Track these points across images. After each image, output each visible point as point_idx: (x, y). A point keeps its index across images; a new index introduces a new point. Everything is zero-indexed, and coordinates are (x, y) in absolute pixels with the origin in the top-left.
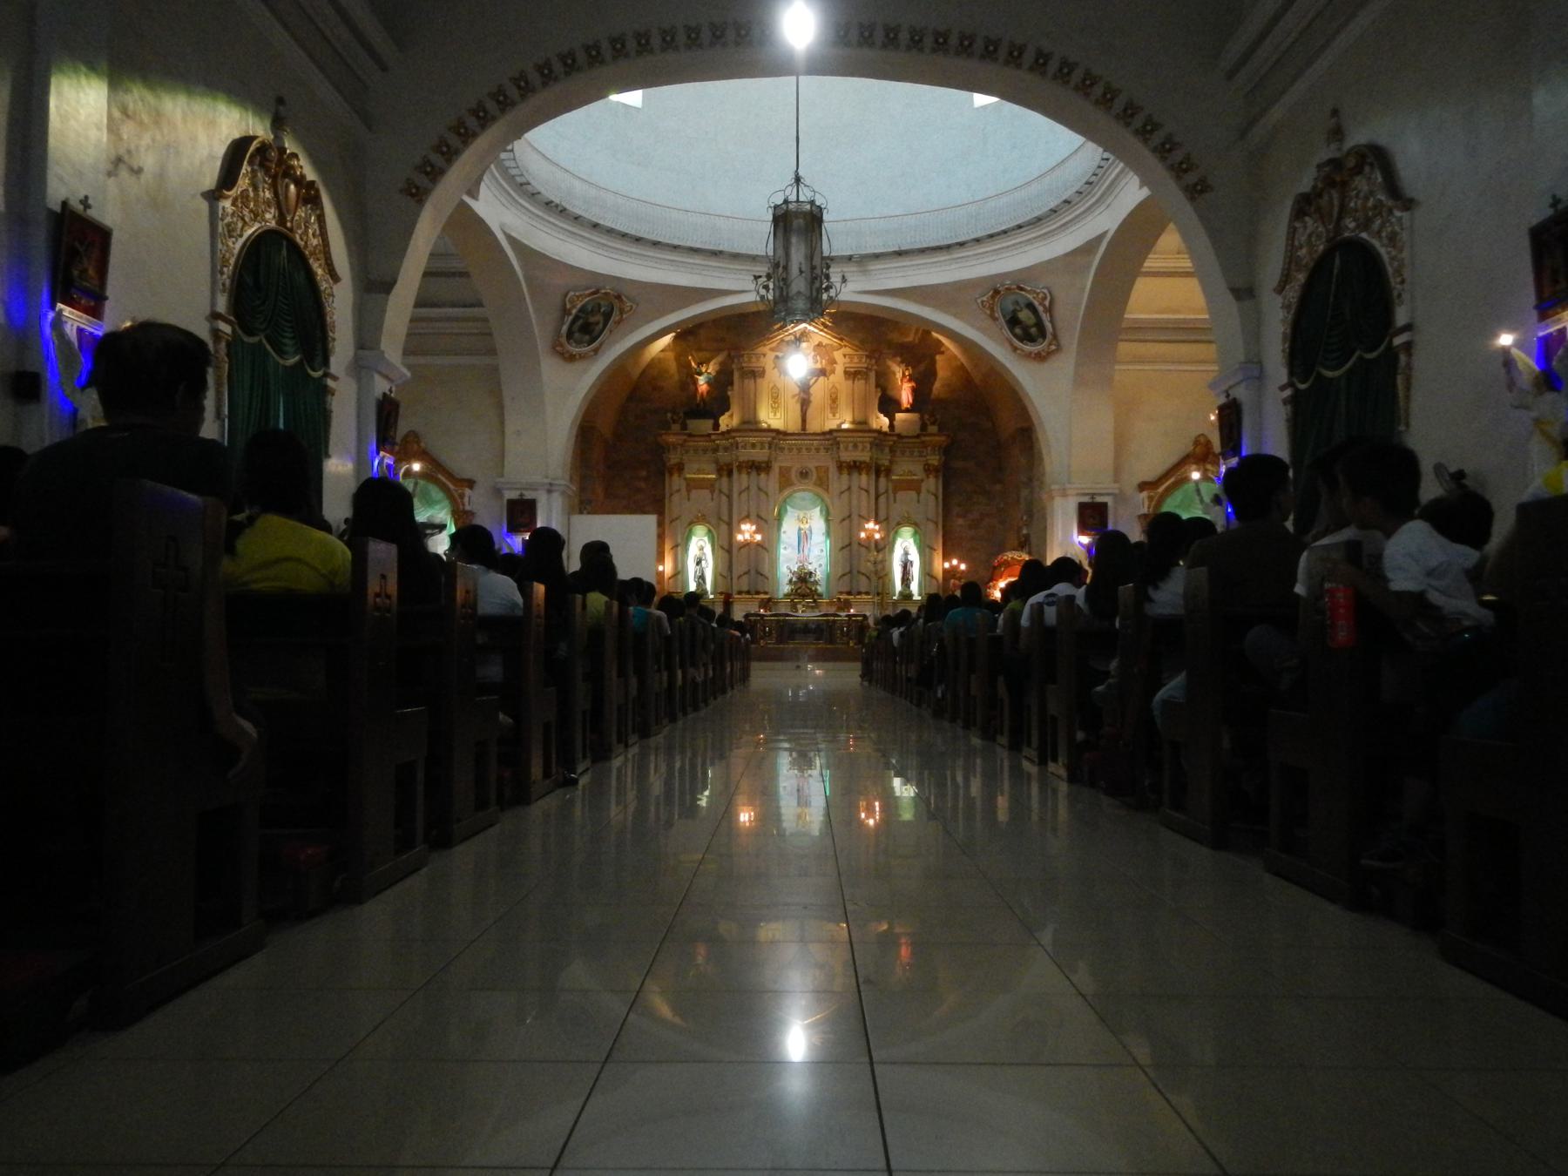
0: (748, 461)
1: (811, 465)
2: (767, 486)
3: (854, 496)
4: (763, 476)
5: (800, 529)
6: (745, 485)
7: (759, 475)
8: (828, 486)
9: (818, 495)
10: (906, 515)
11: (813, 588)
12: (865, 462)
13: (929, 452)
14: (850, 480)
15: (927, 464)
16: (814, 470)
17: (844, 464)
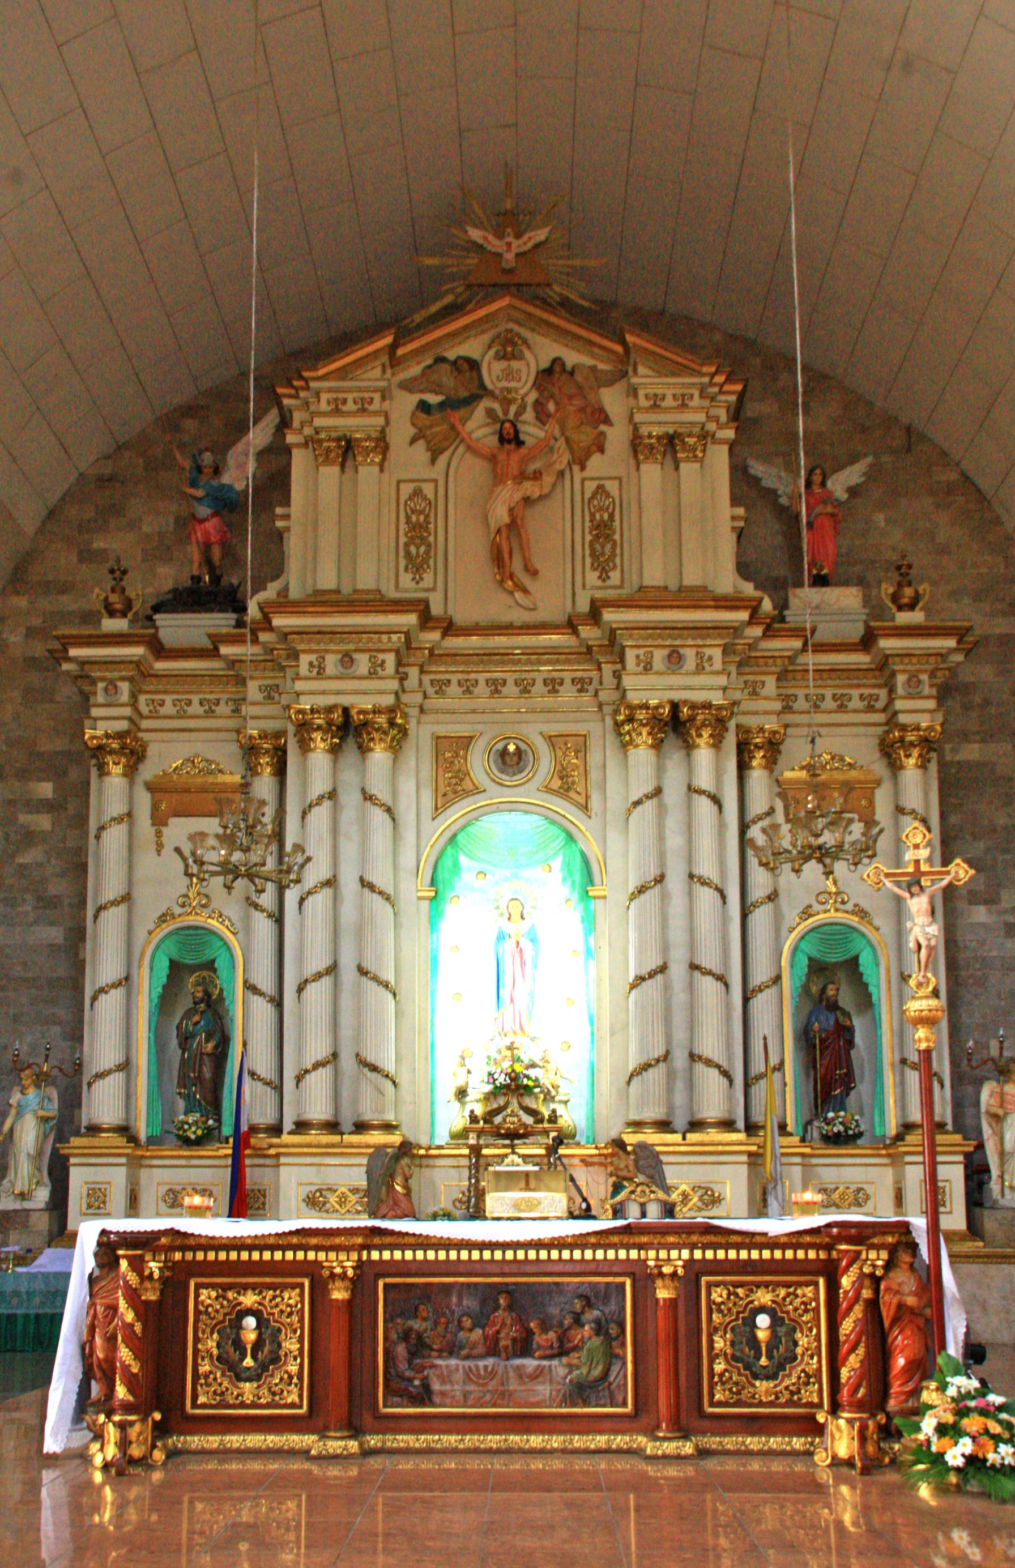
0: (330, 709)
1: (534, 733)
2: (395, 793)
3: (673, 822)
4: (379, 756)
5: (501, 937)
6: (319, 786)
7: (364, 750)
8: (587, 797)
9: (553, 819)
10: (834, 890)
11: (546, 1114)
12: (707, 706)
13: (900, 691)
14: (660, 770)
15: (904, 728)
16: (543, 748)
17: (641, 715)
